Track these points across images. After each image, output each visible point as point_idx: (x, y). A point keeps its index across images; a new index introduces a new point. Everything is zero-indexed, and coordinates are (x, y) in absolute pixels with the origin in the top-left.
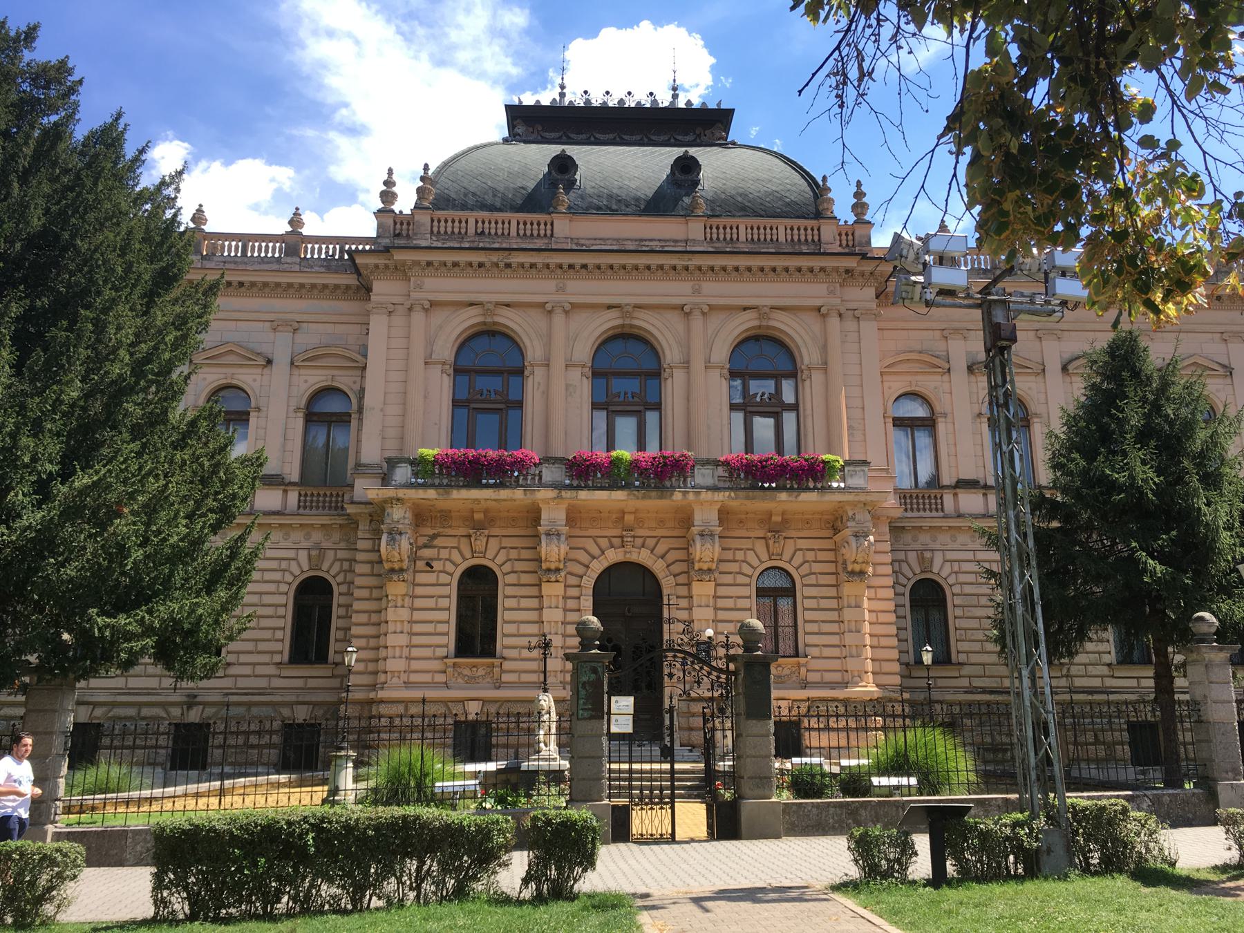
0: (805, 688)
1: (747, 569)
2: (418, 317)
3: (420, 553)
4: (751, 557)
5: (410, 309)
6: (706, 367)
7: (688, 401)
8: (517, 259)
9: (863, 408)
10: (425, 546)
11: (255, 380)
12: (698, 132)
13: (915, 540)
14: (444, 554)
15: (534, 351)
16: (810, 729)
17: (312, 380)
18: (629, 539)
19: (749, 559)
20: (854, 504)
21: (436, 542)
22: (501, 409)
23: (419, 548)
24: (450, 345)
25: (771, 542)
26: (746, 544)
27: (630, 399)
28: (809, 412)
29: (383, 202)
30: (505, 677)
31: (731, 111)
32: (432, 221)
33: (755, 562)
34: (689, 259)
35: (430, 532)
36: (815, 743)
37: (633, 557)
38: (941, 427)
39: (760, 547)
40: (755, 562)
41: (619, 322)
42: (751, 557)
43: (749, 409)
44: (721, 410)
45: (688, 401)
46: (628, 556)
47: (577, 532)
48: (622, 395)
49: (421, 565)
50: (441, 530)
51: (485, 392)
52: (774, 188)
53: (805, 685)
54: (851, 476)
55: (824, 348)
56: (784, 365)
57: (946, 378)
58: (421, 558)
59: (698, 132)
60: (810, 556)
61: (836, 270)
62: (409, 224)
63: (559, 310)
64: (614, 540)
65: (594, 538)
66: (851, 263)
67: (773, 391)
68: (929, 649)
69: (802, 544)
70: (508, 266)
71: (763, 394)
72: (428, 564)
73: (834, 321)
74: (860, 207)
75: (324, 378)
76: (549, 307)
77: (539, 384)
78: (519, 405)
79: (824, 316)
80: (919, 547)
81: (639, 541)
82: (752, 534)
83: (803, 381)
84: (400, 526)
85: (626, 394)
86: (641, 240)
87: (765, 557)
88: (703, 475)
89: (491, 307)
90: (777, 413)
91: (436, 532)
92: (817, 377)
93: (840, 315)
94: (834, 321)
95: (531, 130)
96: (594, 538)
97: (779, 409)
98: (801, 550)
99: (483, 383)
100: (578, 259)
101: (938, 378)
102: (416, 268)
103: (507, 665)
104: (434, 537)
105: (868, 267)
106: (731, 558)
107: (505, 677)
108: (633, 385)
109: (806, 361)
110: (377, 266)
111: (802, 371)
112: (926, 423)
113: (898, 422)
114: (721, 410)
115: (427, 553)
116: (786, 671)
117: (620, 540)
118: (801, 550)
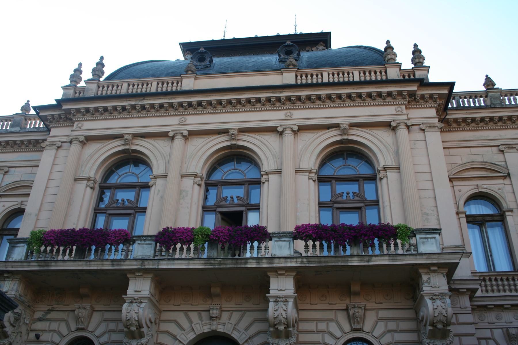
2: (75, 147)
3: (34, 326)
4: (333, 328)
5: (71, 142)
6: (297, 172)
7: (280, 198)
8: (148, 102)
9: (435, 198)
10: (40, 320)
13: (498, 319)
14: (54, 326)
15: (158, 168)
17: (8, 205)
18: (215, 311)
19: (331, 330)
20: (427, 266)
21: (49, 316)
22: (129, 214)
24: (95, 167)
25: (351, 312)
26: (330, 315)
27: (236, 201)
28: (387, 203)
31: (329, 34)
32: (99, 87)
33: (338, 334)
34: (281, 92)
35: (46, 308)
37: (221, 329)
38: (510, 219)
39: (342, 318)
40: (338, 334)
41: (228, 144)
42: (333, 328)
43: (336, 206)
44: (309, 204)
45: (280, 198)
46: (214, 328)
47: (170, 306)
48: (229, 198)
49: (32, 336)
50: (55, 306)
51: (120, 201)
52: (353, 59)
54: (423, 243)
55: (397, 153)
56: (364, 170)
57: (507, 181)
58: (33, 330)
60: (392, 325)
61: (400, 93)
62: (84, 92)
63: (178, 137)
64: (203, 314)
65: (186, 312)
66: (413, 88)
67: (357, 191)
69: (383, 314)
70: (143, 107)
71: (348, 194)
72: (38, 337)
73: (402, 132)
74: (417, 53)
75: (16, 203)
76: (171, 134)
77: (159, 191)
78: (144, 210)
79: (394, 129)
80: (504, 325)
81: (225, 316)
82: (335, 307)
83: (381, 179)
85: (232, 197)
87: (347, 327)
88: (280, 247)
89: (130, 137)
90: (360, 208)
91: (50, 307)
92: (392, 175)
93: (408, 127)
94: (402, 132)
97: (362, 205)
98: (382, 320)
99: (122, 195)
100: (194, 99)
101: (501, 181)
102: (79, 115)
105: (427, 92)
108: (239, 192)
109: (382, 163)
110: (53, 115)
111: (379, 172)
112: (495, 218)
113: (470, 219)
114: (309, 204)
115: (39, 325)
117: (207, 313)
118: (382, 320)
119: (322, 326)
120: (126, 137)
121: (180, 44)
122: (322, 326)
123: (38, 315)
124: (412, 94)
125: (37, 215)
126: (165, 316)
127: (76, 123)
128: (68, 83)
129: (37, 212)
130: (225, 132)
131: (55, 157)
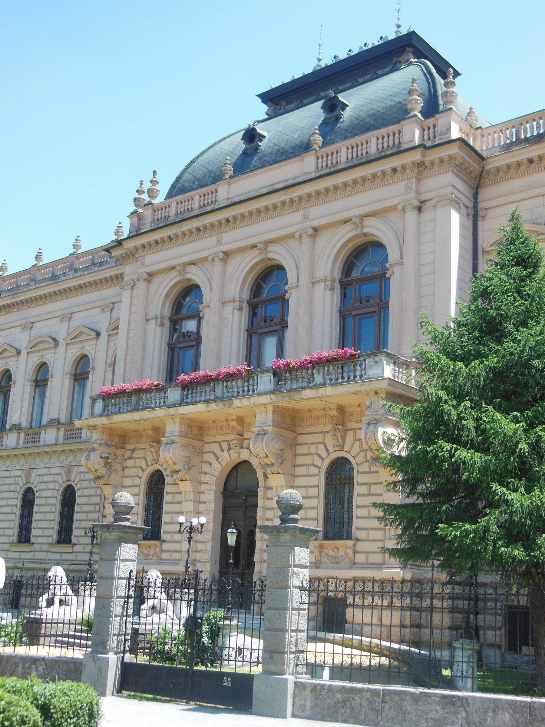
0: (351, 568)
1: (318, 461)
10: (130, 458)
11: (93, 349)
12: (394, 61)
14: (138, 463)
16: (354, 606)
19: (319, 452)
23: (126, 460)
29: (136, 206)
30: (165, 556)
34: (293, 192)
36: (358, 619)
53: (353, 565)
59: (394, 61)
68: (234, 531)
84: (94, 446)
86: (271, 185)
95: (279, 107)
96: (219, 443)
103: (166, 546)
104: (133, 450)
106: (306, 452)
107: (165, 556)
116: (341, 553)
119: (313, 449)
120: (178, 268)
121: (259, 96)
122: (313, 449)
123: (128, 454)
124: (420, 165)
125: (125, 359)
126: (207, 448)
127: (140, 259)
128: (133, 208)
129: (124, 357)
130: (254, 246)
131: (132, 297)
